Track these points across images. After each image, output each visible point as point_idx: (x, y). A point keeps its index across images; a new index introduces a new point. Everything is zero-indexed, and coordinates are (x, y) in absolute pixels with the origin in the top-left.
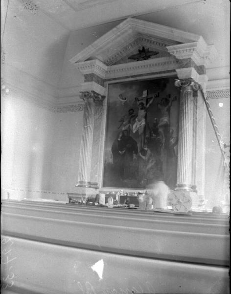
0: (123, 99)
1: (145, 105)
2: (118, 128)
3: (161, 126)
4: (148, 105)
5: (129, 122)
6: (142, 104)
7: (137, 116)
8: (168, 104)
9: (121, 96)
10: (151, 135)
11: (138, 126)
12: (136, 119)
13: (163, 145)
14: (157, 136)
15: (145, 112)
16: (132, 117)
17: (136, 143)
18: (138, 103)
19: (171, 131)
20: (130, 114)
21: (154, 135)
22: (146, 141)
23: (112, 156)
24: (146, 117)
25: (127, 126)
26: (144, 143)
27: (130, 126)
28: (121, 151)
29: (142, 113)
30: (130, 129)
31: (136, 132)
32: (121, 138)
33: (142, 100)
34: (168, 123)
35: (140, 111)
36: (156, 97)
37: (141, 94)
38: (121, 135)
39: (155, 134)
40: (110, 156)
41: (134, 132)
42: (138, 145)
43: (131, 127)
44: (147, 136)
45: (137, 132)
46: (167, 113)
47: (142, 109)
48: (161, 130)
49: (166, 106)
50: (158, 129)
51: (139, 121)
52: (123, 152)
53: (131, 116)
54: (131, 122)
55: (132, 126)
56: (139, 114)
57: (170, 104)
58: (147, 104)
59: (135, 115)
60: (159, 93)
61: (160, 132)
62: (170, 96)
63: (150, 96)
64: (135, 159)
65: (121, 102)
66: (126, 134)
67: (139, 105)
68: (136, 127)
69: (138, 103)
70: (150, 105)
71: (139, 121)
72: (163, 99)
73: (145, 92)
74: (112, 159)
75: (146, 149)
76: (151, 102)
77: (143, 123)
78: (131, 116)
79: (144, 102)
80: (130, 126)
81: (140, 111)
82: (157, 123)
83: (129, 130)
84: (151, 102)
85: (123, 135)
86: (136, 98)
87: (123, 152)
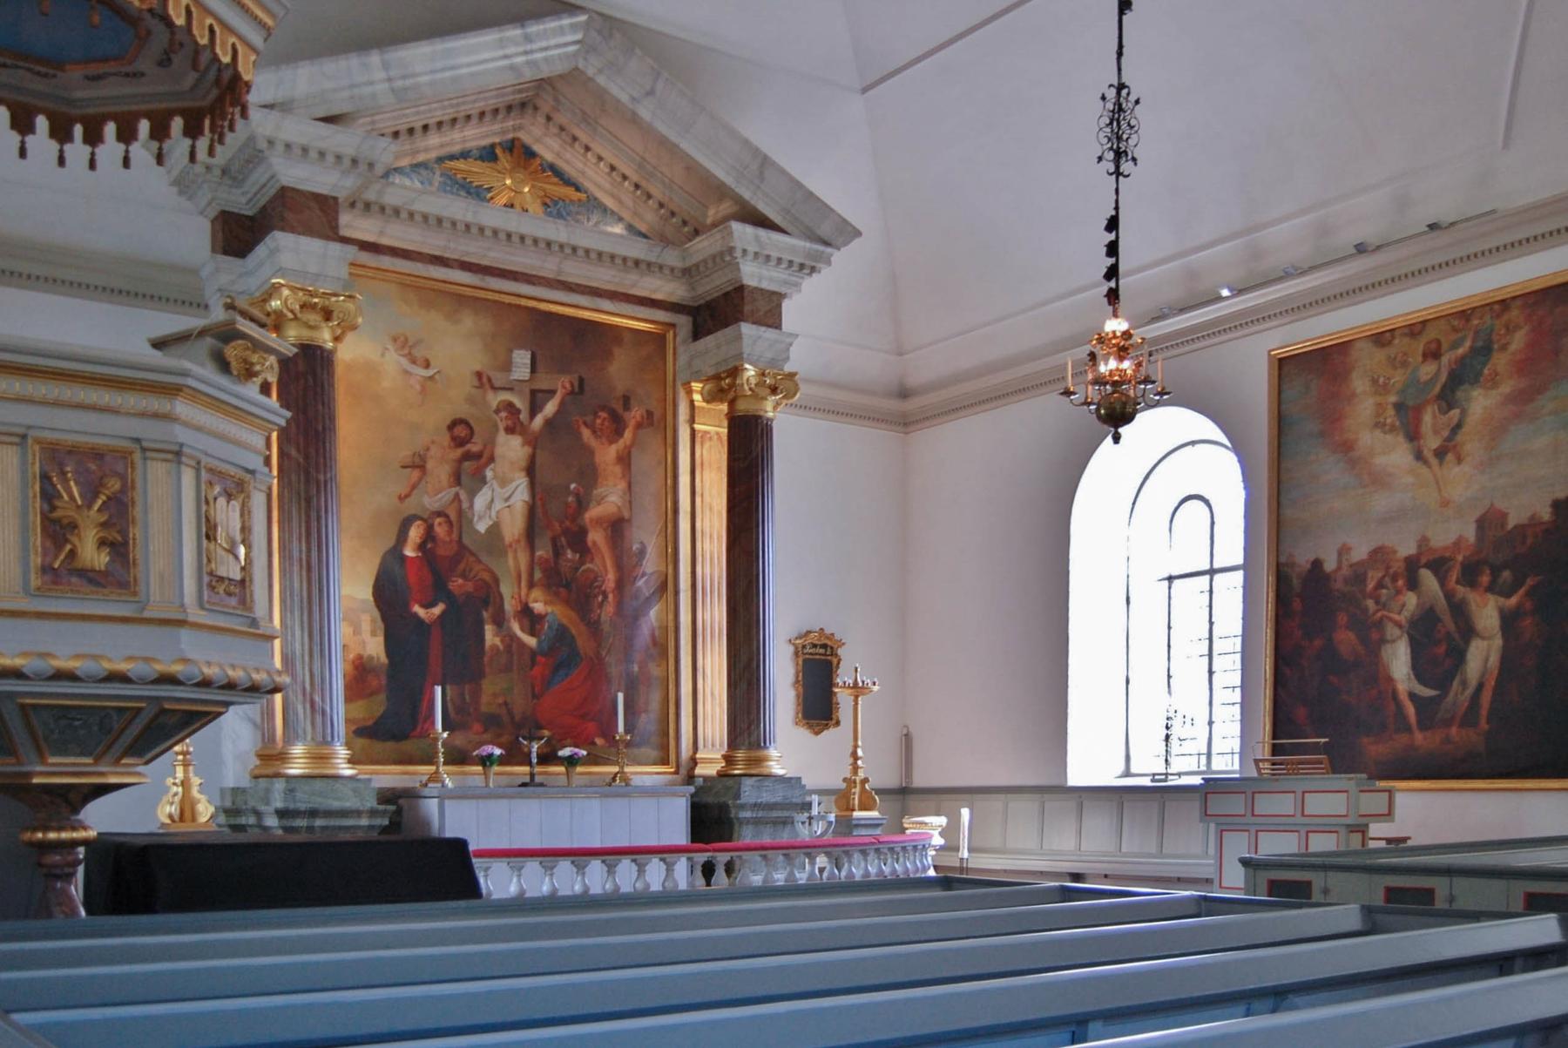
0: (414, 362)
1: (524, 416)
2: (401, 498)
3: (598, 522)
4: (539, 421)
5: (457, 479)
6: (510, 406)
7: (492, 459)
8: (619, 433)
9: (404, 344)
10: (557, 552)
11: (498, 505)
12: (489, 474)
13: (611, 596)
14: (583, 563)
15: (527, 450)
16: (467, 456)
17: (497, 581)
18: (495, 399)
19: (635, 547)
20: (459, 442)
21: (569, 554)
22: (538, 575)
23: (380, 624)
24: (530, 471)
25: (447, 495)
26: (531, 585)
27: (457, 495)
28: (428, 605)
29: (511, 449)
30: (460, 512)
31: (489, 531)
32: (421, 547)
33: (511, 389)
34: (626, 515)
35: (502, 437)
36: (572, 393)
37: (507, 366)
38: (415, 533)
39: (575, 551)
40: (366, 626)
41: (482, 527)
42: (507, 590)
43: (465, 505)
44: (538, 553)
45: (495, 529)
46: (618, 470)
47: (510, 430)
48: (596, 537)
49: (611, 442)
50: (583, 532)
51: (504, 482)
52: (437, 610)
53: (459, 452)
54: (464, 479)
55: (471, 506)
56: (499, 451)
57: (628, 434)
58: (533, 412)
59: (479, 456)
60: (581, 380)
61: (594, 543)
62: (626, 401)
63: (543, 383)
64: (494, 647)
65: (406, 372)
66: (440, 530)
67: (497, 411)
68: (489, 507)
69: (495, 399)
70: (548, 423)
71: (504, 482)
72: (603, 408)
73: (522, 358)
74: (380, 639)
75: (538, 607)
76: (550, 408)
77: (520, 492)
78: (459, 452)
79: (520, 403)
80: (457, 495)
81: (502, 437)
82: (582, 504)
83: (459, 519)
84: (550, 408)
85: (429, 535)
86: (479, 375)
87: (437, 610)
